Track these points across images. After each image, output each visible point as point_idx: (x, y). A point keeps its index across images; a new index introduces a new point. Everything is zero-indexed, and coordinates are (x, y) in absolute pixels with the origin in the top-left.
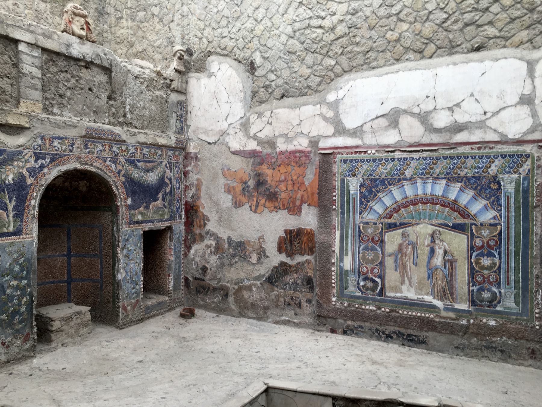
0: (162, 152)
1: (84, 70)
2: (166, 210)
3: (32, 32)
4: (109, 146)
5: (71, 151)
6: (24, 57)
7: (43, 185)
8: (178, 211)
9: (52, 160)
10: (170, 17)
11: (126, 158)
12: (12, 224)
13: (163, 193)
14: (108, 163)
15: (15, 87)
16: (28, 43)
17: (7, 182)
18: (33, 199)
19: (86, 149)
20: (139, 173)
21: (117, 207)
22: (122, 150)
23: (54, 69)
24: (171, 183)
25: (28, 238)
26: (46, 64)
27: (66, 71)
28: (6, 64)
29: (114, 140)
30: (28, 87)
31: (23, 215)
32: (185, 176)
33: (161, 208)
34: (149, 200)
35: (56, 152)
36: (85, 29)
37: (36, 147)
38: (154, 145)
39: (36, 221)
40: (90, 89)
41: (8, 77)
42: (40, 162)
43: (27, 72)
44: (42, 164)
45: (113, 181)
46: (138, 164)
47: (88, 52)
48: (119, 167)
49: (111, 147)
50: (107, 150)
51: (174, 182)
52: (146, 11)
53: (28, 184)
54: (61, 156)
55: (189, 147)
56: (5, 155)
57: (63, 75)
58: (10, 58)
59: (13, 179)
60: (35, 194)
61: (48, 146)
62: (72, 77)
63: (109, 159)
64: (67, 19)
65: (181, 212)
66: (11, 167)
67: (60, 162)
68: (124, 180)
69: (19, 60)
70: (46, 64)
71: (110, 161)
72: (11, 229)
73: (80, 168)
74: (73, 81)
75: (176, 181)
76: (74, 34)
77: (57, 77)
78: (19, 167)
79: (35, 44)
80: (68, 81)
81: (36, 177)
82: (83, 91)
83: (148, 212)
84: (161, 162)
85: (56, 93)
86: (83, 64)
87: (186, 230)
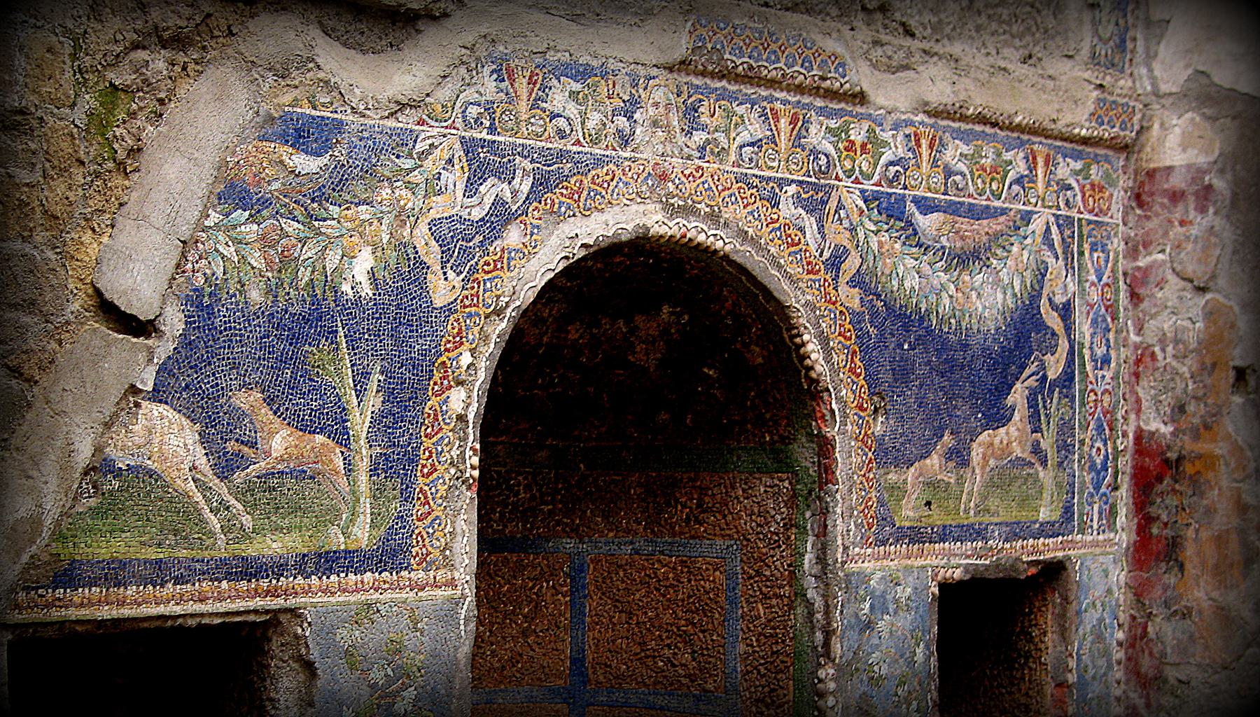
0: (1031, 161)
2: (1045, 476)
4: (793, 121)
5: (625, 140)
7: (498, 312)
8: (1097, 487)
9: (542, 184)
11: (868, 186)
12: (366, 505)
13: (1032, 382)
14: (788, 210)
17: (346, 288)
18: (460, 383)
19: (689, 133)
20: (926, 269)
21: (825, 447)
22: (853, 143)
24: (1069, 329)
25: (436, 585)
29: (816, 91)
31: (413, 461)
32: (1135, 297)
33: (1021, 463)
34: (967, 419)
35: (557, 145)
37: (473, 111)
38: (994, 125)
39: (468, 499)
42: (491, 190)
44: (498, 202)
45: (807, 303)
46: (927, 223)
48: (838, 235)
49: (799, 125)
50: (783, 143)
51: (1084, 328)
53: (438, 303)
54: (582, 166)
55: (1161, 140)
56: (340, 152)
59: (372, 274)
60: (466, 359)
61: (523, 106)
63: (792, 189)
65: (1116, 488)
66: (364, 212)
67: (575, 195)
68: (855, 304)
71: (798, 200)
72: (363, 535)
73: (663, 230)
75: (1094, 322)
78: (402, 217)
81: (473, 271)
83: (960, 481)
84: (1027, 218)
87: (1139, 592)
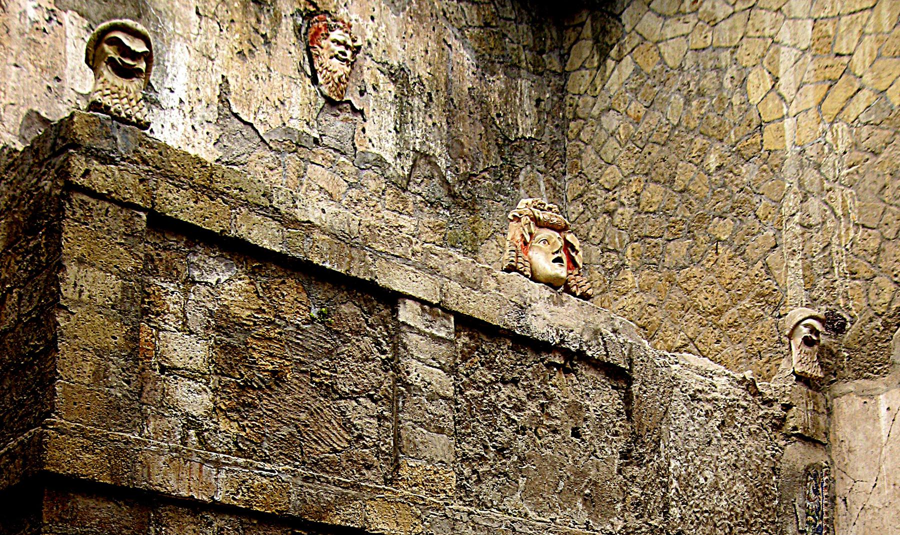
1: (559, 378)
3: (434, 271)
6: (411, 339)
10: (767, 237)
15: (387, 424)
16: (422, 302)
23: (483, 375)
26: (464, 359)
27: (515, 382)
28: (367, 360)
30: (422, 426)
36: (565, 260)
40: (576, 433)
41: (371, 397)
43: (419, 383)
47: (571, 323)
52: (693, 236)
57: (507, 390)
58: (378, 344)
62: (528, 396)
64: (519, 238)
69: (397, 346)
70: (464, 359)
74: (532, 407)
76: (534, 279)
77: (493, 397)
79: (437, 305)
80: (517, 409)
82: (559, 437)
85: (490, 444)
86: (559, 360)
